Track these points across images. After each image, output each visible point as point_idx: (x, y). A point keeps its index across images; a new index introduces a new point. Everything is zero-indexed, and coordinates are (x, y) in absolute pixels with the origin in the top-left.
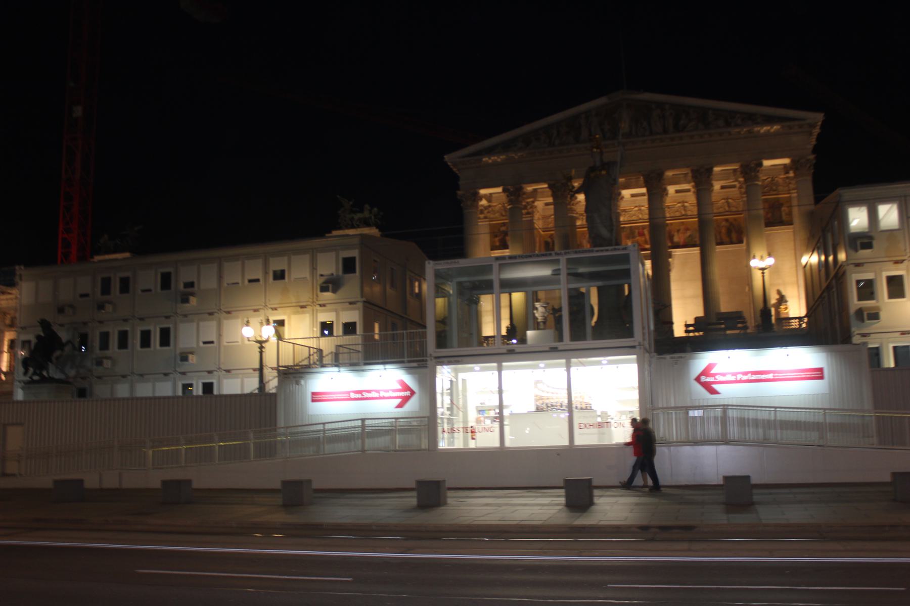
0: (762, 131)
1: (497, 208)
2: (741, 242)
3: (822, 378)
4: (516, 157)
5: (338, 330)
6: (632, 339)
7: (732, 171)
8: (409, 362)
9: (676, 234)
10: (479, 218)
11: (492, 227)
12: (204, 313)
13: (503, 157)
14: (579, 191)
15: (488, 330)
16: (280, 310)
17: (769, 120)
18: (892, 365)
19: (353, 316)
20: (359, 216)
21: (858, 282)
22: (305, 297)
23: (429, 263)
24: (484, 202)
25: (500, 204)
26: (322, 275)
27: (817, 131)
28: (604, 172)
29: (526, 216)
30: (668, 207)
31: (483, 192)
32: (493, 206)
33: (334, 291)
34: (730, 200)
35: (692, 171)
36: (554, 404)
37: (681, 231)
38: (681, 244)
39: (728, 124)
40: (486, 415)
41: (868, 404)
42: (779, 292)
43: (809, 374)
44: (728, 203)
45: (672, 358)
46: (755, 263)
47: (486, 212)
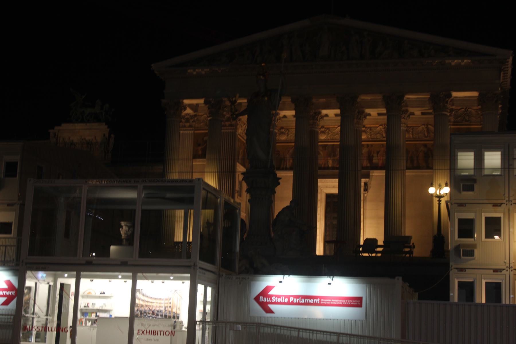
0: (453, 64)
3: (360, 306)
9: (375, 155)
14: (242, 114)
15: (179, 237)
17: (461, 53)
18: (484, 301)
24: (189, 111)
29: (230, 128)
31: (186, 102)
32: (199, 116)
34: (429, 126)
36: (147, 312)
40: (88, 317)
43: (349, 302)
44: (428, 129)
47: (191, 121)
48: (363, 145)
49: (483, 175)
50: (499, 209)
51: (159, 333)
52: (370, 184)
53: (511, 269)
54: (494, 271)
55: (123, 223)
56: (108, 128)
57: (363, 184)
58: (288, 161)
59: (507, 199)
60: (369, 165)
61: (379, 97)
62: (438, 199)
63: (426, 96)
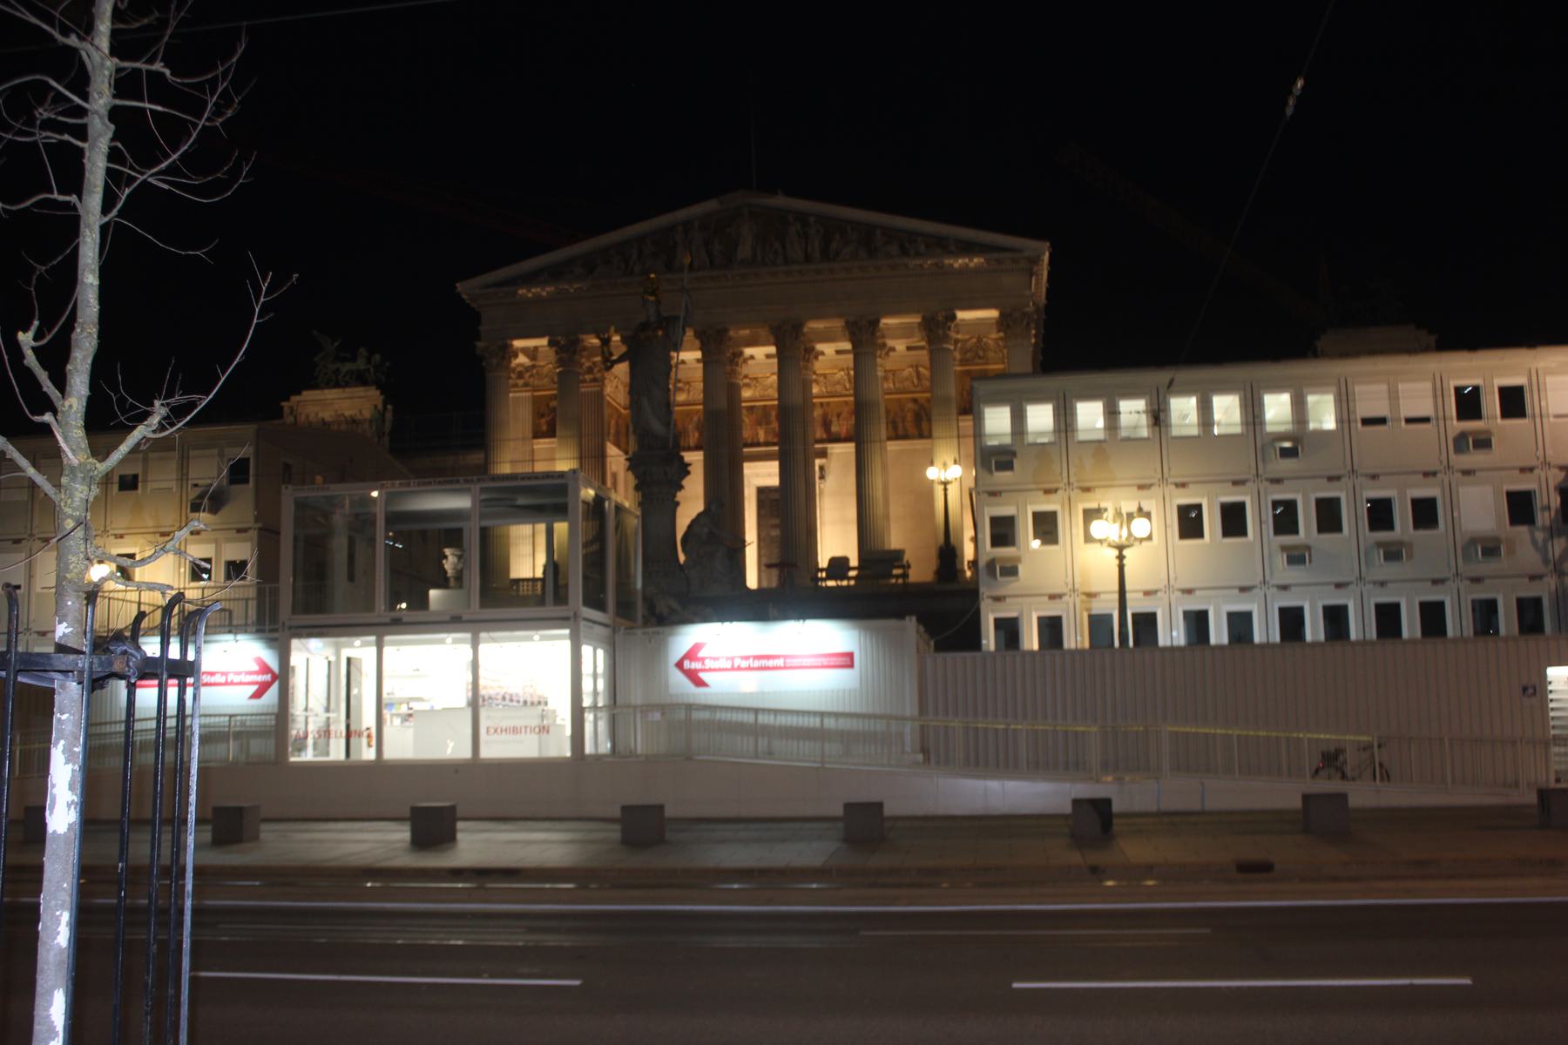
0: (956, 265)
1: (545, 370)
3: (851, 666)
4: (572, 290)
5: (219, 572)
6: (565, 608)
7: (916, 325)
8: (271, 631)
11: (536, 400)
12: (8, 540)
13: (550, 289)
16: (127, 539)
17: (968, 248)
18: (1036, 646)
19: (242, 550)
20: (348, 367)
22: (169, 519)
23: (286, 488)
24: (522, 359)
25: (551, 363)
26: (196, 485)
28: (660, 333)
29: (593, 384)
31: (518, 344)
34: (921, 369)
36: (493, 696)
38: (843, 436)
39: (904, 252)
40: (394, 711)
41: (910, 708)
43: (834, 661)
44: (918, 374)
45: (644, 633)
47: (527, 375)
48: (814, 404)
50: (1053, 497)
51: (523, 730)
53: (1076, 593)
55: (447, 551)
56: (381, 394)
57: (817, 468)
58: (691, 437)
59: (1065, 480)
60: (825, 436)
61: (837, 324)
63: (915, 319)
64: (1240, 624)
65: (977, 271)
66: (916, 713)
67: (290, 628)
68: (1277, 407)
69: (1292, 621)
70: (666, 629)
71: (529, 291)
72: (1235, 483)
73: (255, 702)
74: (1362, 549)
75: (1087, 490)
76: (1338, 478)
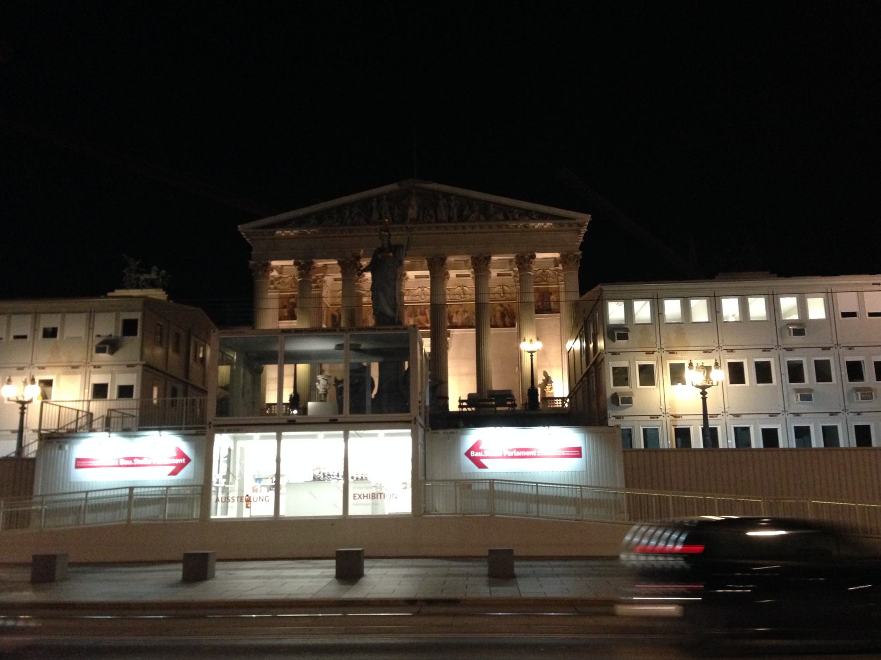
0: (536, 227)
1: (287, 280)
2: (513, 326)
3: (580, 456)
4: (309, 233)
5: (112, 393)
6: (408, 414)
7: (508, 261)
8: (186, 429)
9: (455, 315)
10: (270, 289)
14: (366, 270)
15: (271, 397)
16: (48, 370)
17: (544, 217)
19: (130, 379)
20: (144, 277)
21: (614, 369)
22: (78, 356)
24: (275, 273)
25: (291, 276)
26: (99, 336)
27: (584, 230)
28: (391, 254)
30: (449, 289)
31: (274, 263)
32: (283, 278)
33: (112, 352)
34: (504, 287)
35: (472, 258)
37: (459, 313)
39: (507, 218)
41: (620, 482)
42: (545, 374)
43: (568, 453)
45: (444, 433)
46: (525, 346)
49: (634, 324)
50: (652, 356)
51: (379, 495)
52: (451, 342)
53: (667, 415)
54: (651, 418)
59: (659, 347)
62: (530, 354)
64: (770, 436)
65: (547, 231)
66: (624, 486)
67: (215, 426)
68: (788, 305)
69: (802, 433)
70: (459, 431)
71: (283, 232)
72: (764, 350)
73: (173, 477)
74: (785, 394)
75: (672, 352)
76: (829, 348)
